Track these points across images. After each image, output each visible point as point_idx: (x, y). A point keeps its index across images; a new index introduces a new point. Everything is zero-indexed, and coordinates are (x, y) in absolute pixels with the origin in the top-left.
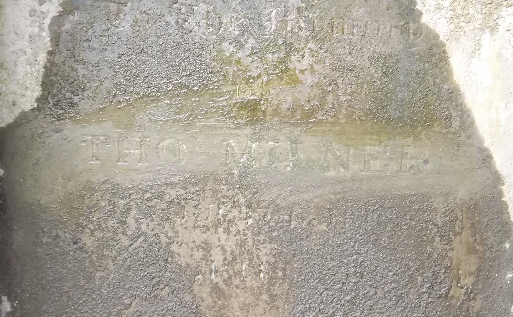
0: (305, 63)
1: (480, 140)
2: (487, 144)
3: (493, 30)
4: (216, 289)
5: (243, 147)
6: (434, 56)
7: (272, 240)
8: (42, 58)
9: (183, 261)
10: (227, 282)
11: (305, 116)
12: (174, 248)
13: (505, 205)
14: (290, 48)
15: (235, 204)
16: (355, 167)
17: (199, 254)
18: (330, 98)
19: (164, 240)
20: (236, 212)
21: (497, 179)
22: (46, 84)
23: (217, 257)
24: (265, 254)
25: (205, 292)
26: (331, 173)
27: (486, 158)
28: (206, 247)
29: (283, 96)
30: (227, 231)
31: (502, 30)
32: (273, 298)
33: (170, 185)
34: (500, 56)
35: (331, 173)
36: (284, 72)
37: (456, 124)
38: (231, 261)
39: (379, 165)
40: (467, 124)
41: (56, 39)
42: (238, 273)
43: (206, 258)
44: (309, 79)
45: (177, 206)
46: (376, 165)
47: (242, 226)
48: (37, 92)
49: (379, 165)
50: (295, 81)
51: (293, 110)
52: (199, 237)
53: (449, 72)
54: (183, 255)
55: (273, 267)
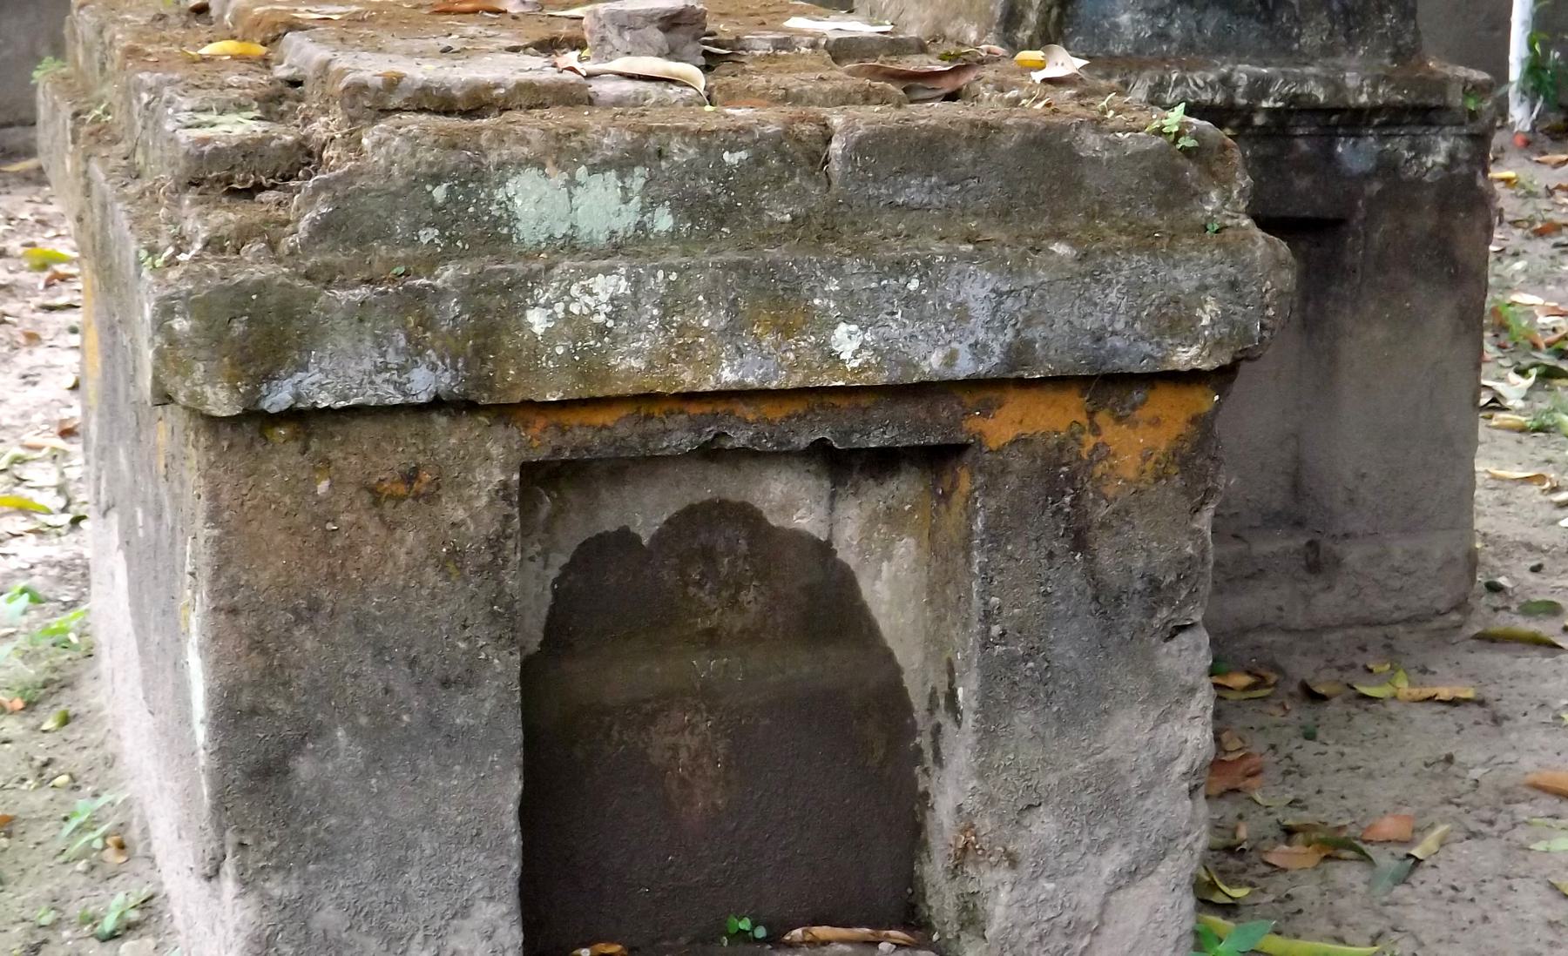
0: (750, 597)
1: (884, 641)
2: (890, 643)
3: (890, 559)
4: (683, 782)
5: (705, 666)
6: (846, 581)
7: (728, 736)
8: (545, 611)
9: (655, 760)
10: (692, 774)
11: (752, 636)
12: (649, 751)
13: (905, 690)
14: (739, 587)
15: (698, 710)
16: (791, 672)
17: (668, 754)
18: (770, 621)
19: (641, 745)
20: (698, 718)
21: (898, 671)
22: (548, 631)
23: (684, 755)
24: (721, 747)
25: (674, 785)
26: (772, 679)
27: (889, 656)
28: (675, 748)
29: (736, 622)
30: (692, 733)
31: (896, 560)
32: (728, 783)
33: (647, 701)
34: (895, 577)
35: (772, 679)
36: (734, 603)
37: (865, 631)
38: (695, 757)
39: (806, 667)
40: (873, 630)
41: (555, 593)
42: (701, 766)
43: (675, 757)
44: (753, 608)
45: (652, 718)
46: (806, 669)
47: (703, 727)
48: (539, 637)
49: (806, 667)
50: (743, 611)
51: (742, 632)
52: (669, 740)
53: (859, 592)
54: (657, 756)
55: (728, 758)
